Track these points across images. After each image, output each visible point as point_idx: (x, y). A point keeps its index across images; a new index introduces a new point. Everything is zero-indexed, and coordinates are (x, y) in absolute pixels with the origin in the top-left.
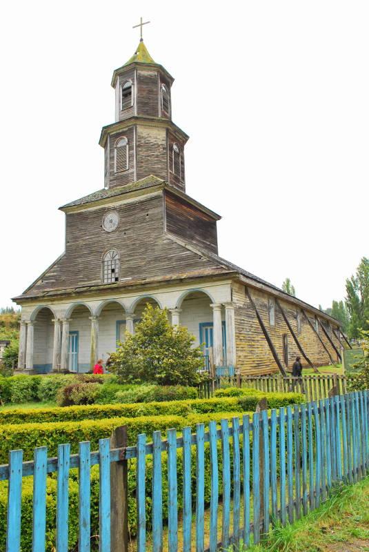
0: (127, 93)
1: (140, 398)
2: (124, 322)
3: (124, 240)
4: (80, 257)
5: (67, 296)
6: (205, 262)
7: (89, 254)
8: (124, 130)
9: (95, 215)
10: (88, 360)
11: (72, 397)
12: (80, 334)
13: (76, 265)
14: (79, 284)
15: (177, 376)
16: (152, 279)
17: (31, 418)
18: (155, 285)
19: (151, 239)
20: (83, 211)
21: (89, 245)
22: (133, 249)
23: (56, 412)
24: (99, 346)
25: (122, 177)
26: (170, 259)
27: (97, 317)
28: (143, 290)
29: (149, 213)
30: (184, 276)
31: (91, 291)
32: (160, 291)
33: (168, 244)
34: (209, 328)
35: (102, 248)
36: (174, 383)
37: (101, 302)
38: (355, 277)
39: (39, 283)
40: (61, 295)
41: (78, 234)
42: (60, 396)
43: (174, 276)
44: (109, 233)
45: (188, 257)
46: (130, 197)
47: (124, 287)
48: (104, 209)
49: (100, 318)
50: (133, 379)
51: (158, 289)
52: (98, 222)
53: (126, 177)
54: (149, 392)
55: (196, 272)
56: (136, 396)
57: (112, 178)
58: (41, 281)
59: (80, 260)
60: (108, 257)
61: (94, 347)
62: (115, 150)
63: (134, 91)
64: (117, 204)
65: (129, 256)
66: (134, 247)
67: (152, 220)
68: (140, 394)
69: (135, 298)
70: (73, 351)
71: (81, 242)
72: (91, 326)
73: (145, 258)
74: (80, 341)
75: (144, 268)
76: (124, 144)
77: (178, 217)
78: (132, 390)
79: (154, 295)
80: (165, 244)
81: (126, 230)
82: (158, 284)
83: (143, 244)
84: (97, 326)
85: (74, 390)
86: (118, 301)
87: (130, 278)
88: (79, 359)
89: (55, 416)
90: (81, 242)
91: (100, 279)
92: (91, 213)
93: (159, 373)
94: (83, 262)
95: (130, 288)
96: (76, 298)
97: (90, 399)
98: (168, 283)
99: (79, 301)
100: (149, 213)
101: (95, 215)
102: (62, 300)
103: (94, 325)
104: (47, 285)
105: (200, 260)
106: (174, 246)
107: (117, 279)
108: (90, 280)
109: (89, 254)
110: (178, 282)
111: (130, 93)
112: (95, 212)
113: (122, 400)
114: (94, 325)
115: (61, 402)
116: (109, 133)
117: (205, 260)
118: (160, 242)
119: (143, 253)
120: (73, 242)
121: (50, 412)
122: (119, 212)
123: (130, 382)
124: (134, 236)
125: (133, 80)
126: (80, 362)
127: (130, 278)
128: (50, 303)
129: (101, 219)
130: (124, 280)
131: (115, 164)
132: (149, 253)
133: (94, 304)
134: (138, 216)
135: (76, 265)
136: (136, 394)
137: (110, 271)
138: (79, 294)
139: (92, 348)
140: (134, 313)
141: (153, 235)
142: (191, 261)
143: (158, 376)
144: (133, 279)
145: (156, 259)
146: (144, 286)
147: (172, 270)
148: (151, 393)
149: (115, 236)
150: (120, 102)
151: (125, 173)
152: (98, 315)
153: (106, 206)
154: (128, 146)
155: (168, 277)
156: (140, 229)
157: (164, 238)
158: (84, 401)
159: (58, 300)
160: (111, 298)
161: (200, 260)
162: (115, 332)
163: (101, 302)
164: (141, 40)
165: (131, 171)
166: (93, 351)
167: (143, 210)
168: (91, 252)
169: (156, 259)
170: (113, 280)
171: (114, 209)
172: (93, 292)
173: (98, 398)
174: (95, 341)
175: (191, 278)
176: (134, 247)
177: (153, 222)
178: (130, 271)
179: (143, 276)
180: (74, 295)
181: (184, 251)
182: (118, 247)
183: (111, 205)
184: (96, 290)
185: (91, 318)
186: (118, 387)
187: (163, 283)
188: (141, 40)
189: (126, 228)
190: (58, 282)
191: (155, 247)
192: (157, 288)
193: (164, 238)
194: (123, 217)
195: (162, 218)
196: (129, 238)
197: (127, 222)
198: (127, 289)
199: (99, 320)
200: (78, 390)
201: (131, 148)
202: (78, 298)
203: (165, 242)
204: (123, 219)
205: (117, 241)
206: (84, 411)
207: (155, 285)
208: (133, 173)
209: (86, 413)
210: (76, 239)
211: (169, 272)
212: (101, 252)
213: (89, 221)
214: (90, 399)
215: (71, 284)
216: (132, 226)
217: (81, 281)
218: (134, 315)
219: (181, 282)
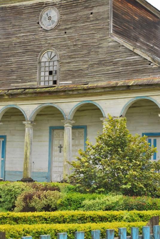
1: (107, 207)
2: (62, 128)
3: (64, 39)
4: (13, 56)
6: (154, 69)
7: (23, 53)
9: (32, 10)
10: (20, 168)
11: (33, 204)
12: (8, 139)
13: (8, 65)
14: (12, 85)
15: (141, 187)
16: (95, 84)
17: (24, 221)
18: (99, 91)
19: (96, 40)
21: (24, 42)
22: (74, 51)
23: (46, 217)
24: (33, 153)
26: (115, 63)
27: (32, 122)
28: (85, 96)
29: (93, 11)
30: (131, 83)
31: (26, 94)
32: (104, 97)
33: (114, 47)
34: (152, 139)
35: (39, 47)
36: (138, 194)
37: (36, 106)
41: (10, 30)
42: (19, 201)
43: (120, 83)
44: (47, 31)
45: (136, 63)
47: (64, 91)
49: (35, 123)
50: (97, 188)
51: (101, 95)
54: (118, 202)
55: (144, 79)
56: (104, 205)
59: (13, 59)
60: (45, 58)
61: (28, 154)
65: (70, 57)
66: (75, 48)
67: (97, 20)
68: (107, 203)
69: (75, 104)
71: (14, 40)
72: (25, 130)
73: (87, 61)
75: (86, 72)
77: (124, 16)
78: (99, 198)
79: (96, 101)
80: (112, 47)
81: (66, 29)
82: (103, 90)
83: (85, 46)
84: (31, 132)
85: (35, 197)
86: (55, 105)
87: (71, 82)
88: (7, 165)
89: (46, 219)
90: (14, 40)
91: (35, 81)
92: (26, 7)
93: (126, 184)
94: (16, 62)
95: (71, 93)
96: (8, 101)
97: (53, 206)
98: (114, 90)
99: (11, 104)
100: (93, 11)
101: (32, 10)
103: (28, 130)
105: (149, 66)
106: (121, 49)
107: (55, 82)
108: (24, 81)
109: (23, 53)
110: (125, 88)
112: (31, 7)
113: (89, 208)
114: (28, 130)
115: (21, 208)
117: (154, 66)
118: (105, 44)
120: (6, 39)
121: (41, 216)
122: (59, 8)
123: (93, 192)
124: (76, 35)
126: (7, 169)
127: (71, 82)
129: (38, 15)
130: (62, 84)
132: (92, 54)
134: (79, 14)
135: (8, 65)
136: (103, 203)
137: (47, 73)
138: (13, 96)
139: (26, 155)
140: (73, 120)
141: (98, 36)
142: (139, 67)
143: (124, 186)
144: (73, 83)
145: (101, 63)
146: (87, 92)
147: (118, 75)
148: (120, 203)
149: (54, 34)
152: (33, 120)
155: (113, 82)
156: (83, 28)
157: (110, 40)
158: (47, 208)
160: (47, 102)
161: (149, 66)
162: (47, 139)
163: (36, 106)
166: (26, 158)
167: (86, 7)
168: (27, 51)
169: (101, 63)
170: (51, 83)
172: (29, 95)
173: (62, 206)
174: (29, 147)
175: (140, 85)
176: (75, 48)
177: (97, 22)
178: (70, 74)
179: (85, 80)
180: (6, 97)
181: (131, 55)
182: (57, 47)
184: (32, 93)
185: (24, 122)
186: (83, 195)
187: (108, 89)
189: (68, 27)
191: (100, 50)
192: (100, 94)
193: (110, 40)
194: (64, 15)
195: (108, 18)
196: (70, 38)
198: (66, 93)
199: (33, 126)
200: (39, 198)
202: (10, 101)
203: (111, 44)
204: (64, 17)
205: (56, 41)
206: (73, 216)
207: (99, 91)
209: (75, 218)
211: (114, 77)
212: (37, 52)
213: (24, 16)
214: (53, 206)
216: (73, 25)
217: (13, 83)
218: (73, 122)
219: (128, 89)
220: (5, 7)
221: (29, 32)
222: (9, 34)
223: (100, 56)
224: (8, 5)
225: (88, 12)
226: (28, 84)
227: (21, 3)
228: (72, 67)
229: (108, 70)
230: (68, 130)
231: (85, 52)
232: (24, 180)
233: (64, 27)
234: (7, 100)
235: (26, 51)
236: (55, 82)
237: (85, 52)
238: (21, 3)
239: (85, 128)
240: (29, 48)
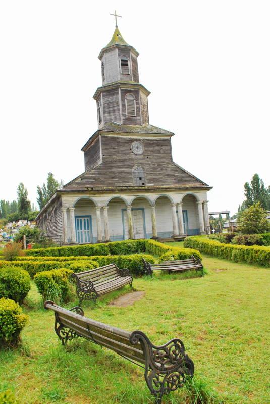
0: (124, 64)
4: (115, 166)
5: (112, 191)
8: (131, 89)
12: (92, 218)
13: (111, 172)
20: (116, 136)
21: (122, 160)
22: (154, 168)
25: (132, 120)
26: (176, 176)
31: (129, 190)
38: (46, 185)
39: (79, 180)
40: (107, 190)
43: (182, 186)
44: (136, 155)
45: (185, 177)
46: (152, 136)
48: (133, 139)
52: (128, 147)
53: (135, 120)
57: (124, 118)
58: (80, 179)
59: (114, 169)
62: (126, 100)
63: (130, 63)
64: (141, 138)
67: (165, 153)
70: (85, 229)
74: (92, 222)
76: (132, 99)
80: (173, 168)
81: (147, 155)
90: (115, 157)
92: (121, 139)
98: (180, 189)
102: (103, 194)
104: (87, 183)
107: (143, 184)
108: (125, 182)
111: (127, 65)
112: (125, 139)
116: (120, 88)
119: (160, 171)
125: (129, 57)
128: (92, 196)
130: (149, 185)
131: (126, 109)
133: (129, 198)
134: (155, 148)
135: (111, 172)
138: (122, 191)
141: (166, 161)
142: (187, 179)
145: (168, 175)
146: (166, 190)
147: (177, 182)
150: (120, 67)
151: (134, 118)
153: (134, 137)
154: (135, 101)
155: (177, 186)
159: (99, 194)
162: (121, 216)
164: (116, 27)
165: (138, 118)
167: (158, 145)
169: (168, 175)
170: (141, 185)
171: (139, 141)
172: (132, 191)
175: (192, 188)
178: (151, 180)
179: (161, 184)
180: (117, 191)
183: (137, 138)
188: (116, 27)
190: (97, 181)
191: (167, 169)
192: (171, 191)
196: (151, 161)
197: (149, 151)
201: (137, 103)
204: (146, 149)
208: (140, 119)
210: (110, 154)
211: (176, 183)
213: (120, 144)
215: (109, 184)
219: (187, 189)
220: (107, 137)
221: (125, 154)
222: (111, 153)
223: (168, 172)
224: (108, 136)
225: (158, 148)
226: (127, 184)
227: (118, 136)
228: (153, 176)
229: (172, 179)
230: (129, 211)
231: (159, 169)
232: (153, 239)
233: (147, 154)
234: (117, 193)
235: (124, 165)
236: (143, 184)
237: (159, 169)
238: (118, 136)
239: (143, 209)
240: (126, 163)
